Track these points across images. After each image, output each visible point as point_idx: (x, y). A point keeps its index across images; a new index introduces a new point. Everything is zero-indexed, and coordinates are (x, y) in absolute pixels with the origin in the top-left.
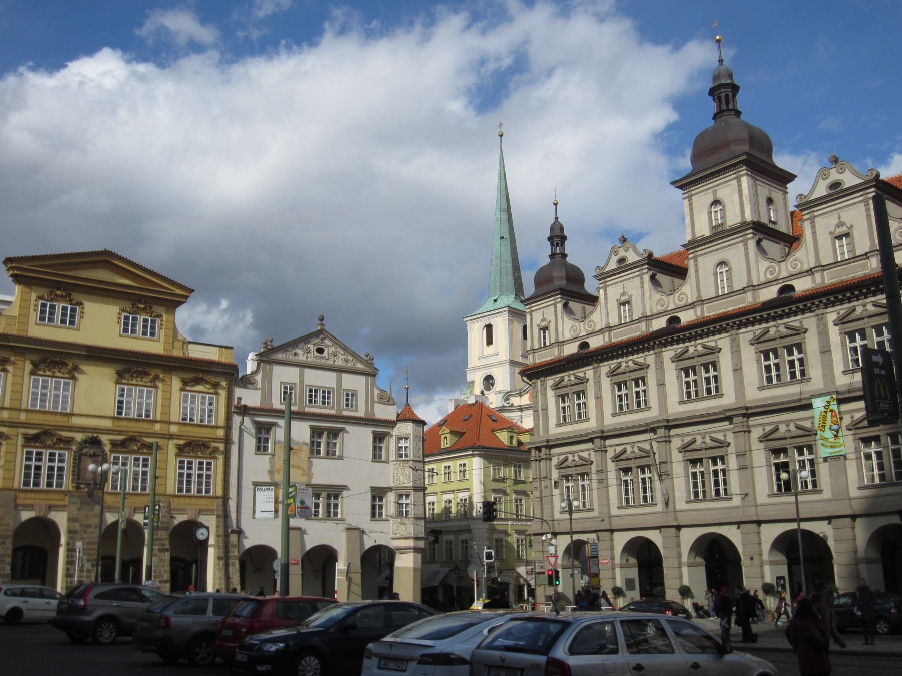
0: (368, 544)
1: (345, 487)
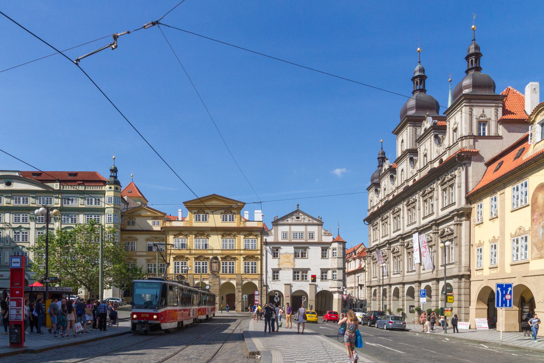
0: (319, 290)
1: (309, 269)
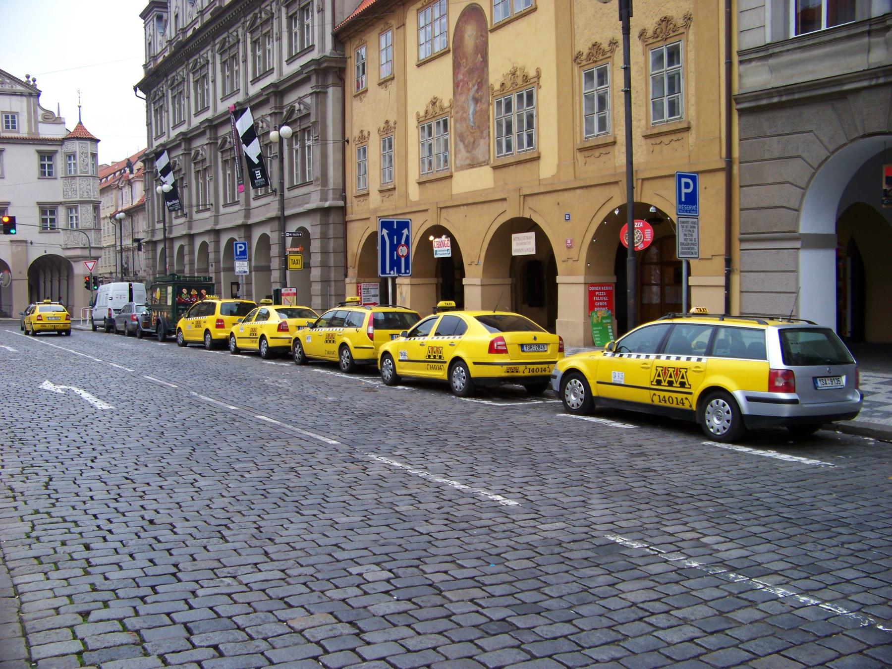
1: (8, 203)
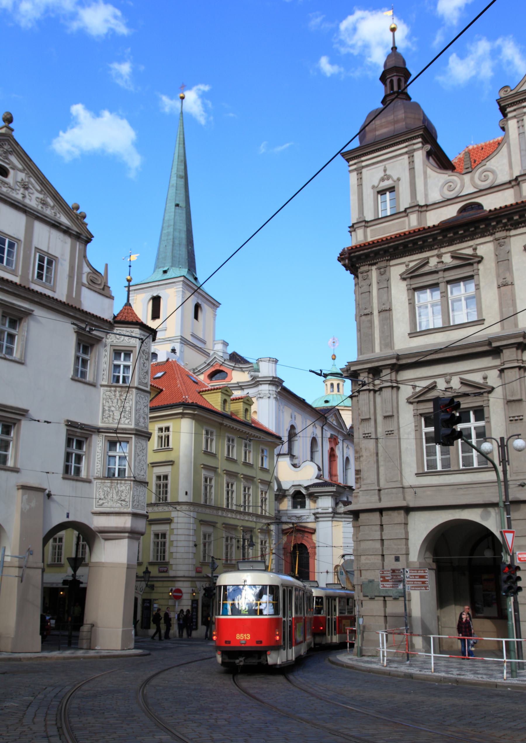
1: (23, 413)
